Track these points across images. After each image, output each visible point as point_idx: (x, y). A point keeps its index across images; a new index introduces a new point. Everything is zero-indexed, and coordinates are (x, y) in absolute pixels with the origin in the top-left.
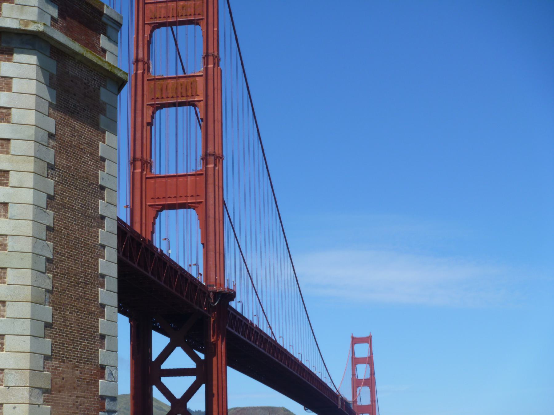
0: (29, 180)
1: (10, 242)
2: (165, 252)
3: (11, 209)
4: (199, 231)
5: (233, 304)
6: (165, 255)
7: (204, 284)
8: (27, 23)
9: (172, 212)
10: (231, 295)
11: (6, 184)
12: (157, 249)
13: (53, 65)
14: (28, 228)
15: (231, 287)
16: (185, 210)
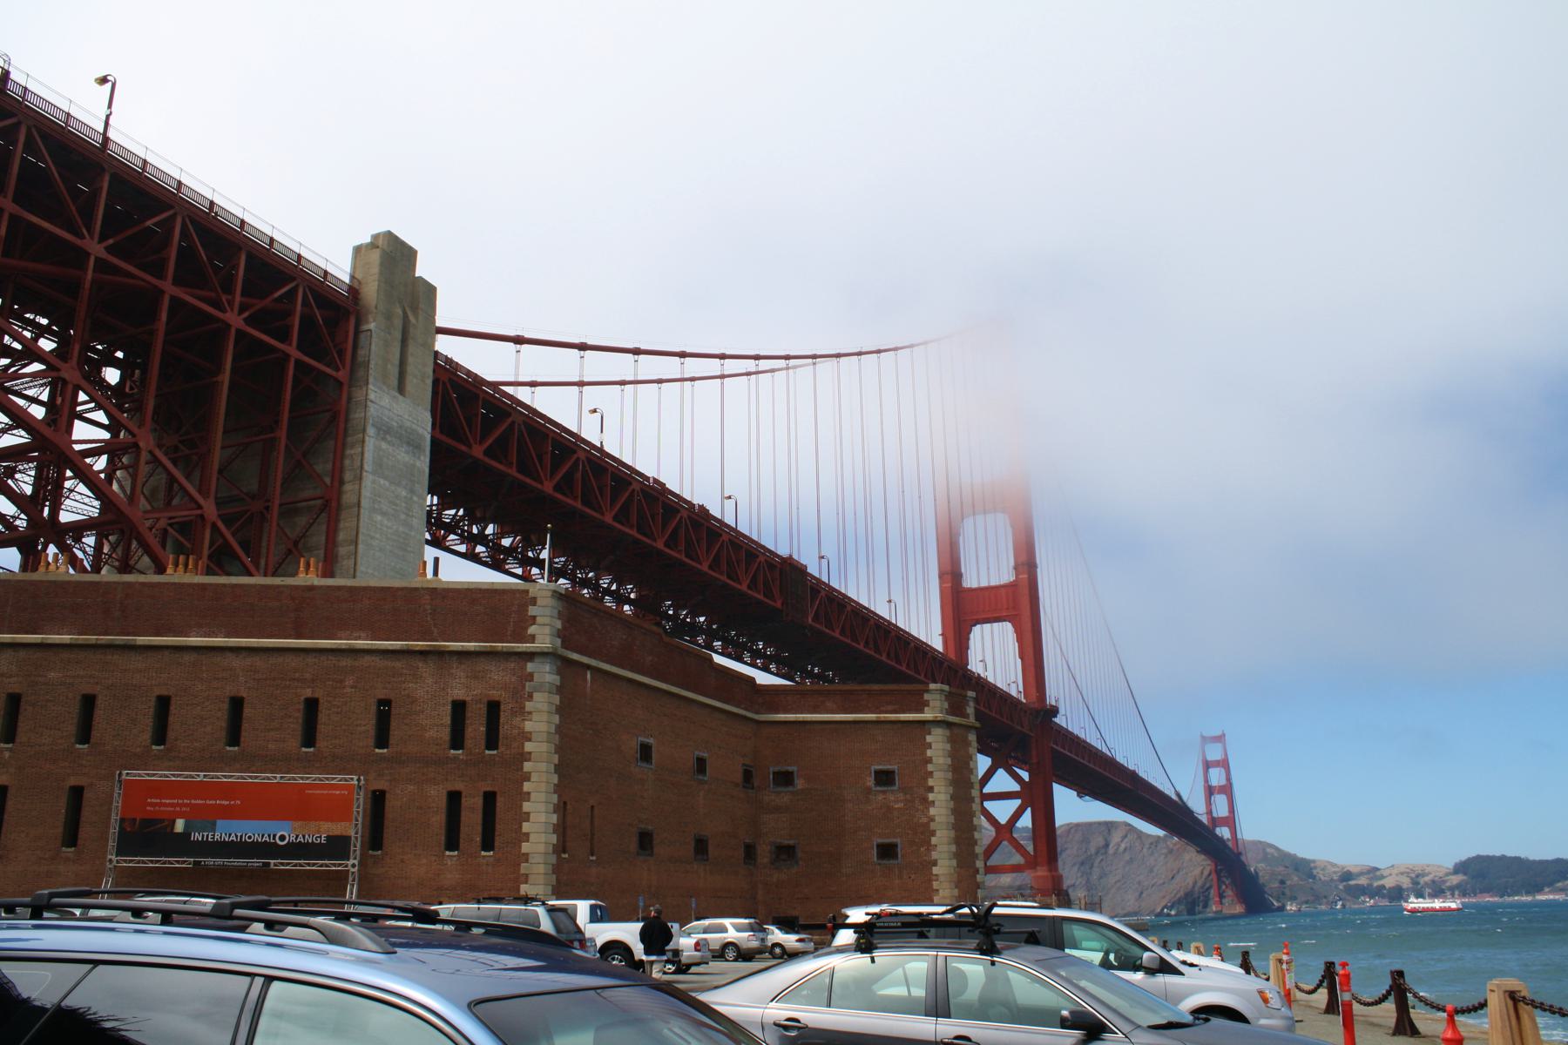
0: (943, 789)
1: (937, 818)
2: (982, 675)
3: (936, 803)
4: (1017, 644)
5: (1057, 720)
6: (982, 678)
7: (1024, 701)
8: (936, 717)
9: (987, 627)
10: (1054, 711)
11: (933, 792)
12: (974, 673)
13: (947, 732)
14: (944, 811)
15: (1054, 703)
16: (1000, 623)
